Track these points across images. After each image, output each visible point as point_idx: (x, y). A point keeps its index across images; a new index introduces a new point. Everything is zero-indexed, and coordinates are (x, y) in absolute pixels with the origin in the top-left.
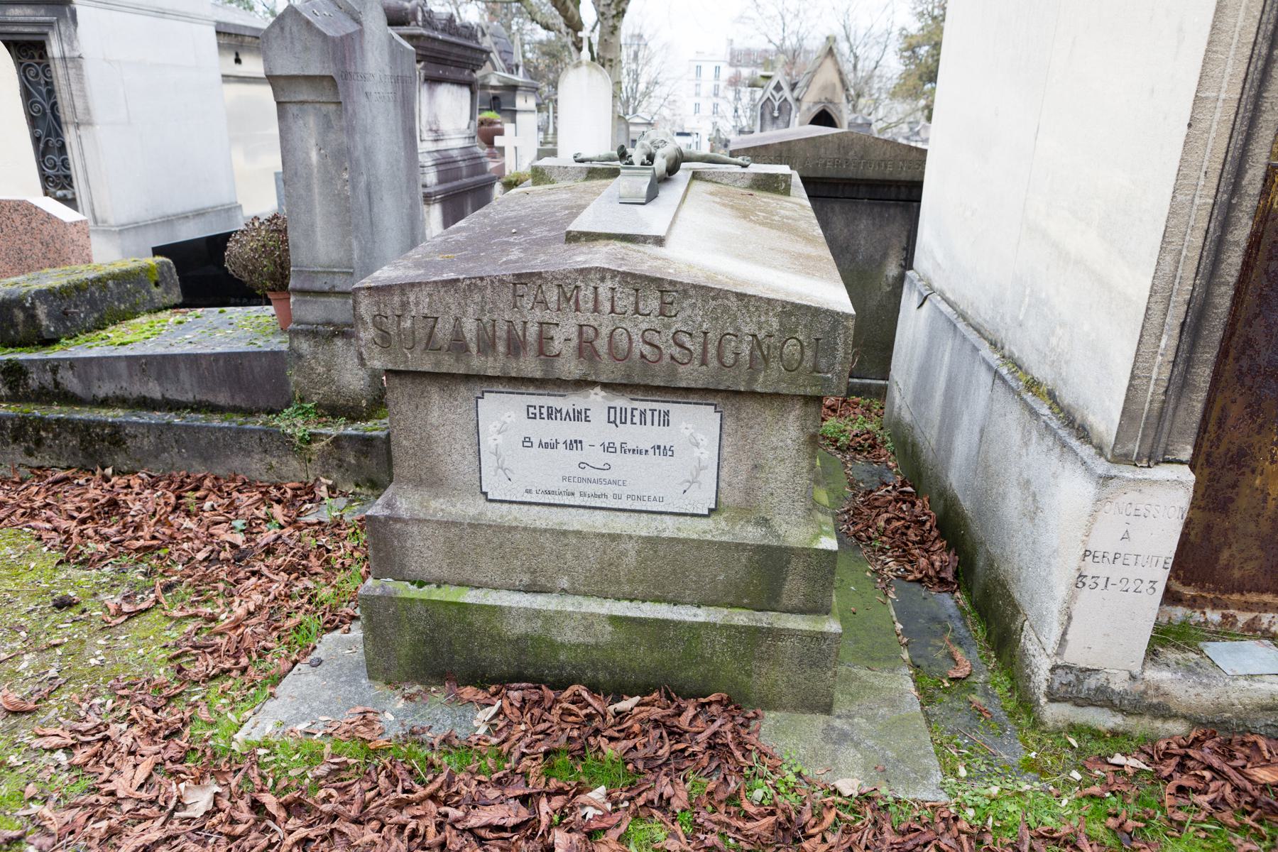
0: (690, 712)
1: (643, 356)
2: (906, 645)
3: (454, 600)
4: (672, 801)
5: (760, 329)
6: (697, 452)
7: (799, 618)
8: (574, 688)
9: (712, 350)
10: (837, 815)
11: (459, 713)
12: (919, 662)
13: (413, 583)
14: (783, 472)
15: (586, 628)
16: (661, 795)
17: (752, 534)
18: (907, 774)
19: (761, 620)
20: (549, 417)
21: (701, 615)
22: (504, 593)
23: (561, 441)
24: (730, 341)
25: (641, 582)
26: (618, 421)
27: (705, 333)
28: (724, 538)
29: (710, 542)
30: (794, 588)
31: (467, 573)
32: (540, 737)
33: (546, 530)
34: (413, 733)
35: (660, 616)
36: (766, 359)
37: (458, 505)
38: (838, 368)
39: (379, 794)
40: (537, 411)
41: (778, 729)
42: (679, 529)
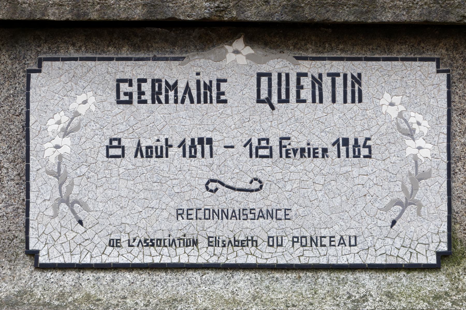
6: (411, 147)
20: (155, 98)
23: (175, 141)
26: (275, 99)
42: (390, 295)
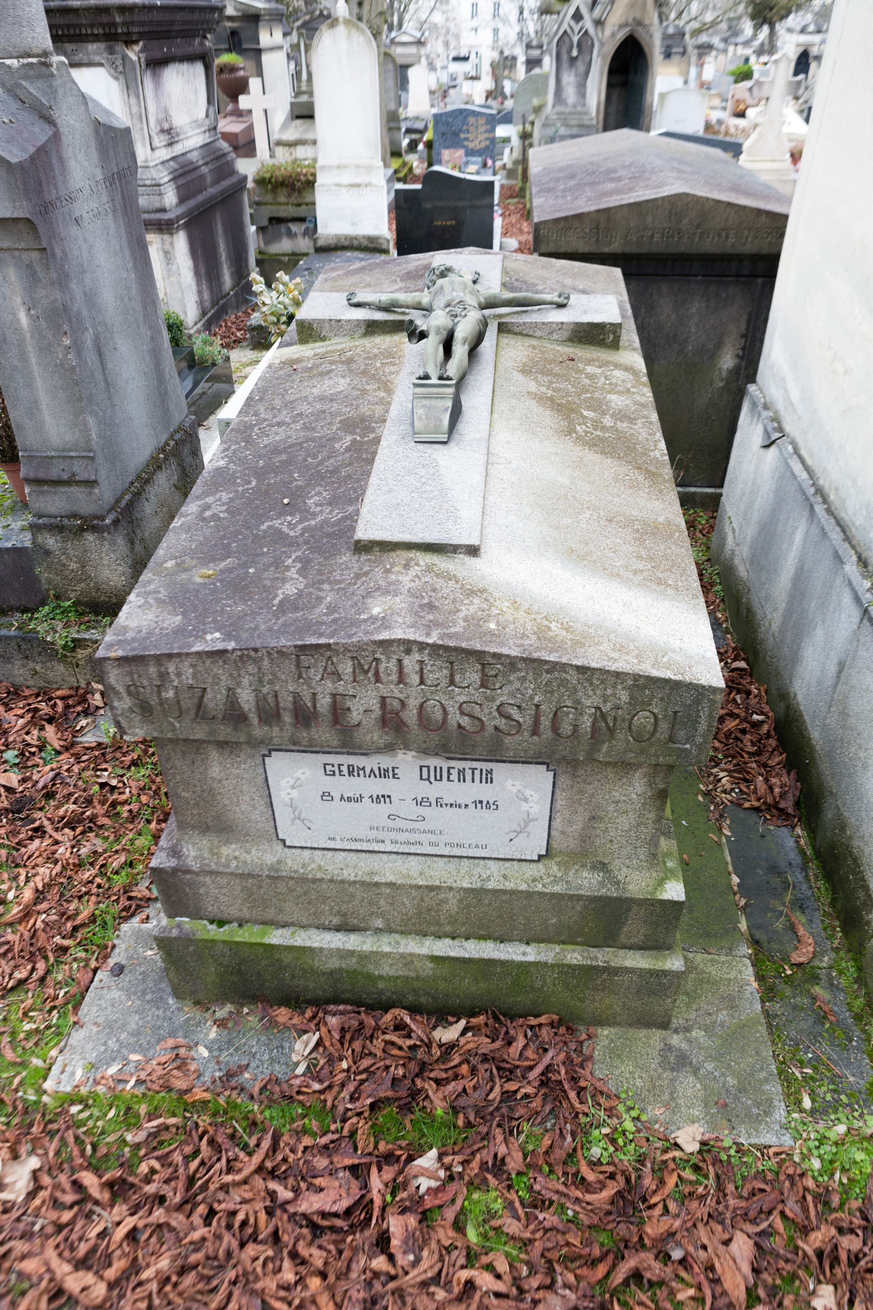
0: (521, 1042)
1: (460, 726)
2: (744, 908)
3: (259, 940)
4: (508, 1160)
5: (605, 702)
6: (525, 807)
7: (638, 954)
8: (396, 1011)
9: (545, 722)
10: (679, 1176)
11: (276, 1043)
12: (758, 935)
13: (212, 922)
14: (624, 822)
15: (405, 965)
16: (496, 1155)
17: (587, 882)
18: (748, 1108)
19: (596, 958)
20: (351, 773)
21: (529, 954)
22: (313, 932)
23: (366, 795)
24: (568, 713)
25: (464, 924)
26: (432, 779)
27: (537, 706)
28: (557, 889)
29: (541, 894)
30: (634, 927)
31: (271, 914)
32: (364, 1076)
33: (355, 882)
34: (230, 1075)
35: (485, 956)
36: (611, 731)
37: (253, 851)
38: (699, 740)
39: (203, 1163)
40: (336, 769)
41: (613, 1053)
42: (505, 877)
